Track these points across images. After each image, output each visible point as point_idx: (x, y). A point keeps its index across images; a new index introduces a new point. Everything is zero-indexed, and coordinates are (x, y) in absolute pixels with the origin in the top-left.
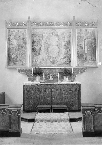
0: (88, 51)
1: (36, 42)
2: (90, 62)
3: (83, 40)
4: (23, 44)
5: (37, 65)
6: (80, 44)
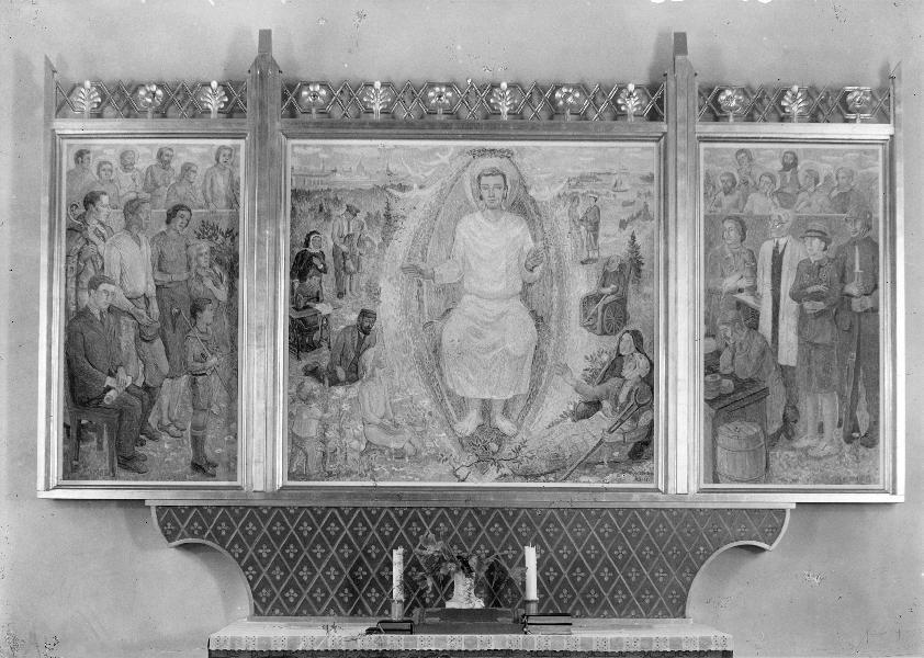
0: (807, 345)
1: (329, 258)
3: (767, 249)
4: (209, 283)
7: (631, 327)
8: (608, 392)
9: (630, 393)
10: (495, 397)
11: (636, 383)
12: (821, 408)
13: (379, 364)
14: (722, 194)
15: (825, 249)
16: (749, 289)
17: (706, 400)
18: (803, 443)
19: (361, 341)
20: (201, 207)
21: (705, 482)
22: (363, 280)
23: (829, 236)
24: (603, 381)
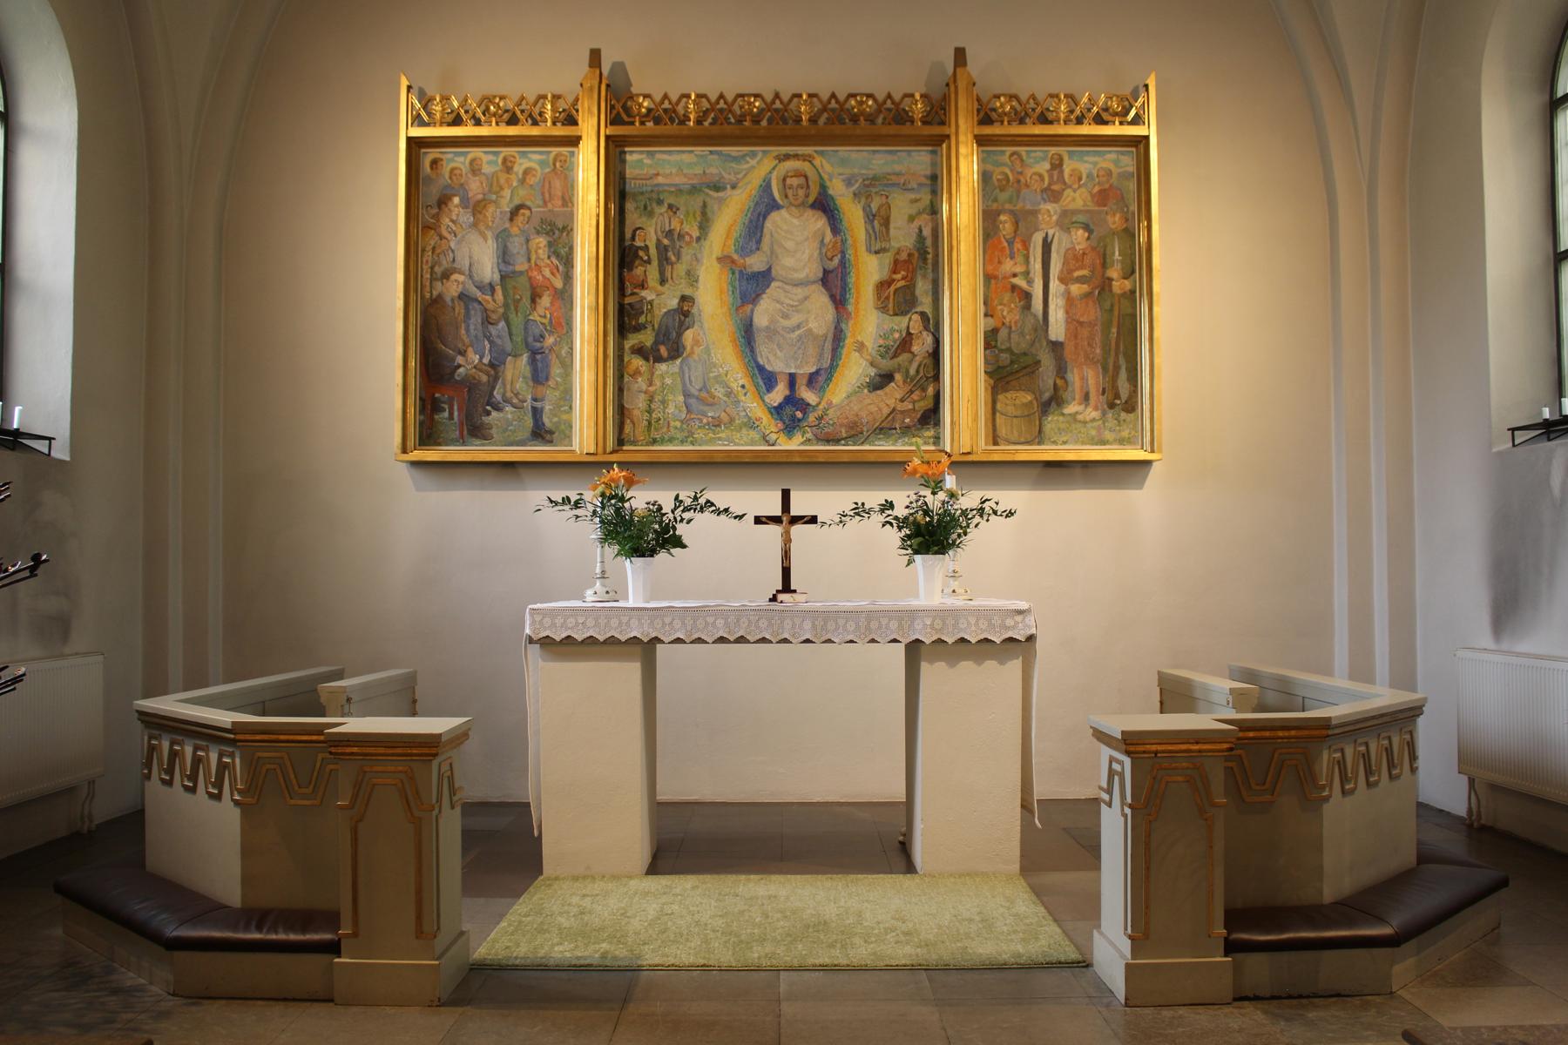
0: (1072, 322)
1: (653, 251)
2: (1091, 413)
3: (1038, 239)
4: (547, 272)
5: (654, 442)
6: (1008, 266)
7: (919, 309)
8: (899, 365)
9: (919, 366)
10: (798, 371)
11: (924, 358)
12: (1085, 377)
13: (697, 342)
14: (998, 190)
15: (1088, 238)
16: (1022, 273)
17: (985, 372)
18: (1071, 409)
19: (681, 323)
20: (539, 207)
21: (986, 445)
22: (681, 269)
23: (1092, 226)
24: (895, 356)
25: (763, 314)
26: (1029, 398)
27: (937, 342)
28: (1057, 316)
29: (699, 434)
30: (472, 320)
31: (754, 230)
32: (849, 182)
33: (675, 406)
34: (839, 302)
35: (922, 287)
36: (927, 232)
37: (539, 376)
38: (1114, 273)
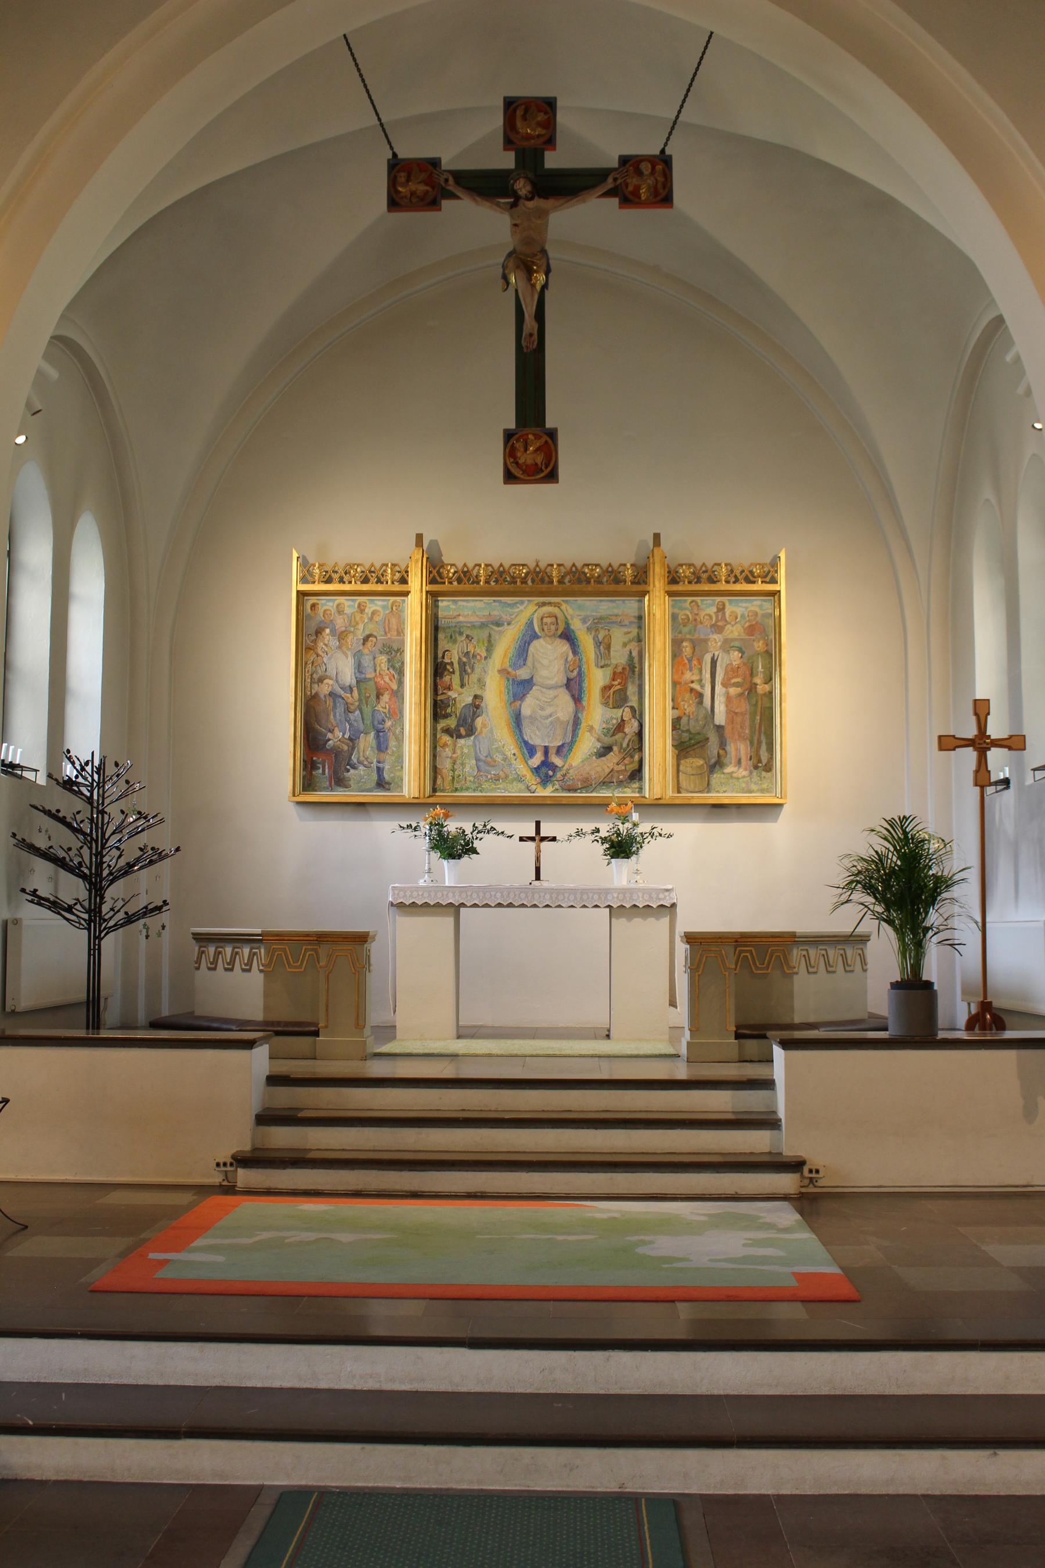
0: (731, 713)
1: (456, 666)
2: (742, 772)
3: (708, 658)
4: (387, 679)
5: (456, 790)
6: (688, 676)
7: (629, 704)
8: (616, 741)
9: (629, 741)
10: (550, 745)
11: (633, 736)
12: (737, 748)
13: (484, 725)
14: (681, 626)
15: (741, 657)
16: (697, 680)
17: (673, 745)
18: (729, 769)
19: (474, 713)
20: (382, 636)
21: (673, 793)
22: (474, 677)
23: (744, 649)
24: (613, 735)
25: (527, 707)
26: (701, 762)
27: (641, 726)
28: (720, 709)
29: (485, 786)
30: (338, 710)
31: (522, 652)
32: (584, 621)
33: (470, 767)
34: (577, 699)
35: (632, 690)
36: (635, 654)
37: (381, 746)
38: (758, 680)
